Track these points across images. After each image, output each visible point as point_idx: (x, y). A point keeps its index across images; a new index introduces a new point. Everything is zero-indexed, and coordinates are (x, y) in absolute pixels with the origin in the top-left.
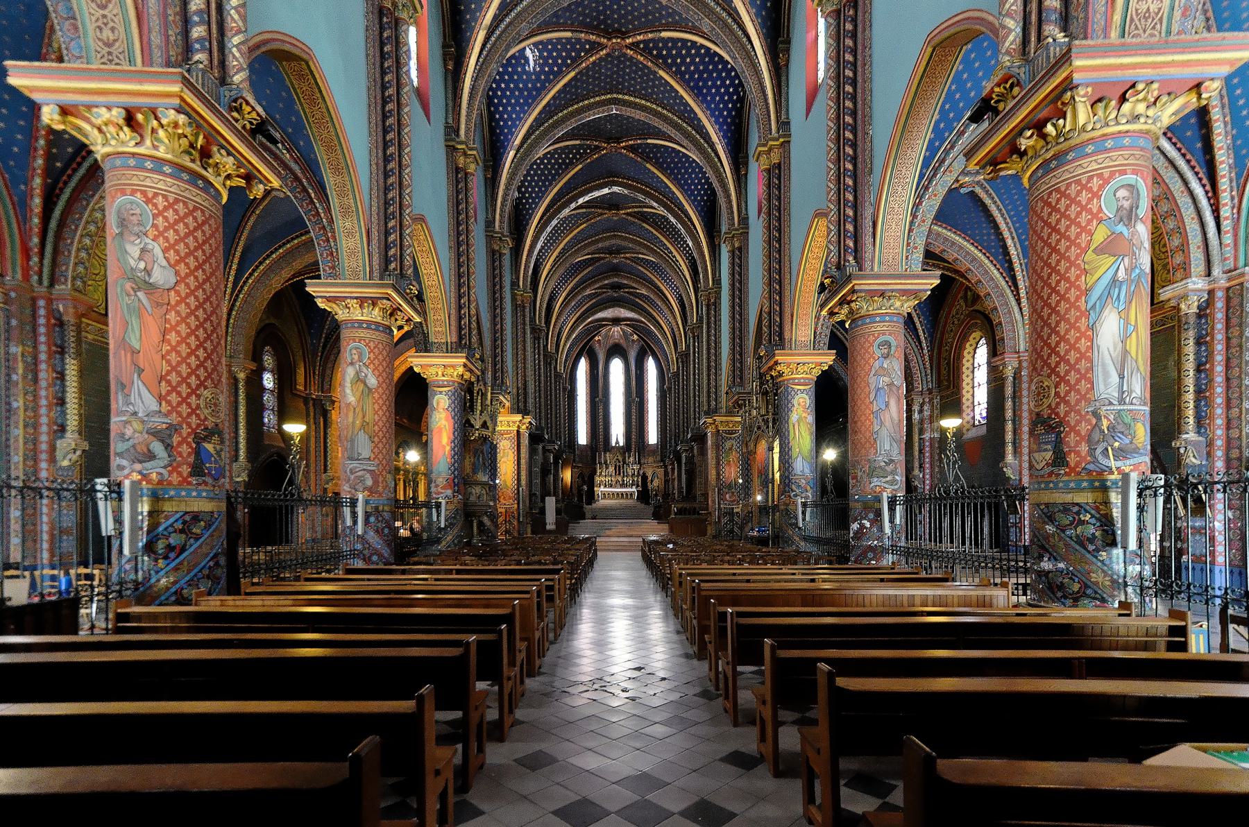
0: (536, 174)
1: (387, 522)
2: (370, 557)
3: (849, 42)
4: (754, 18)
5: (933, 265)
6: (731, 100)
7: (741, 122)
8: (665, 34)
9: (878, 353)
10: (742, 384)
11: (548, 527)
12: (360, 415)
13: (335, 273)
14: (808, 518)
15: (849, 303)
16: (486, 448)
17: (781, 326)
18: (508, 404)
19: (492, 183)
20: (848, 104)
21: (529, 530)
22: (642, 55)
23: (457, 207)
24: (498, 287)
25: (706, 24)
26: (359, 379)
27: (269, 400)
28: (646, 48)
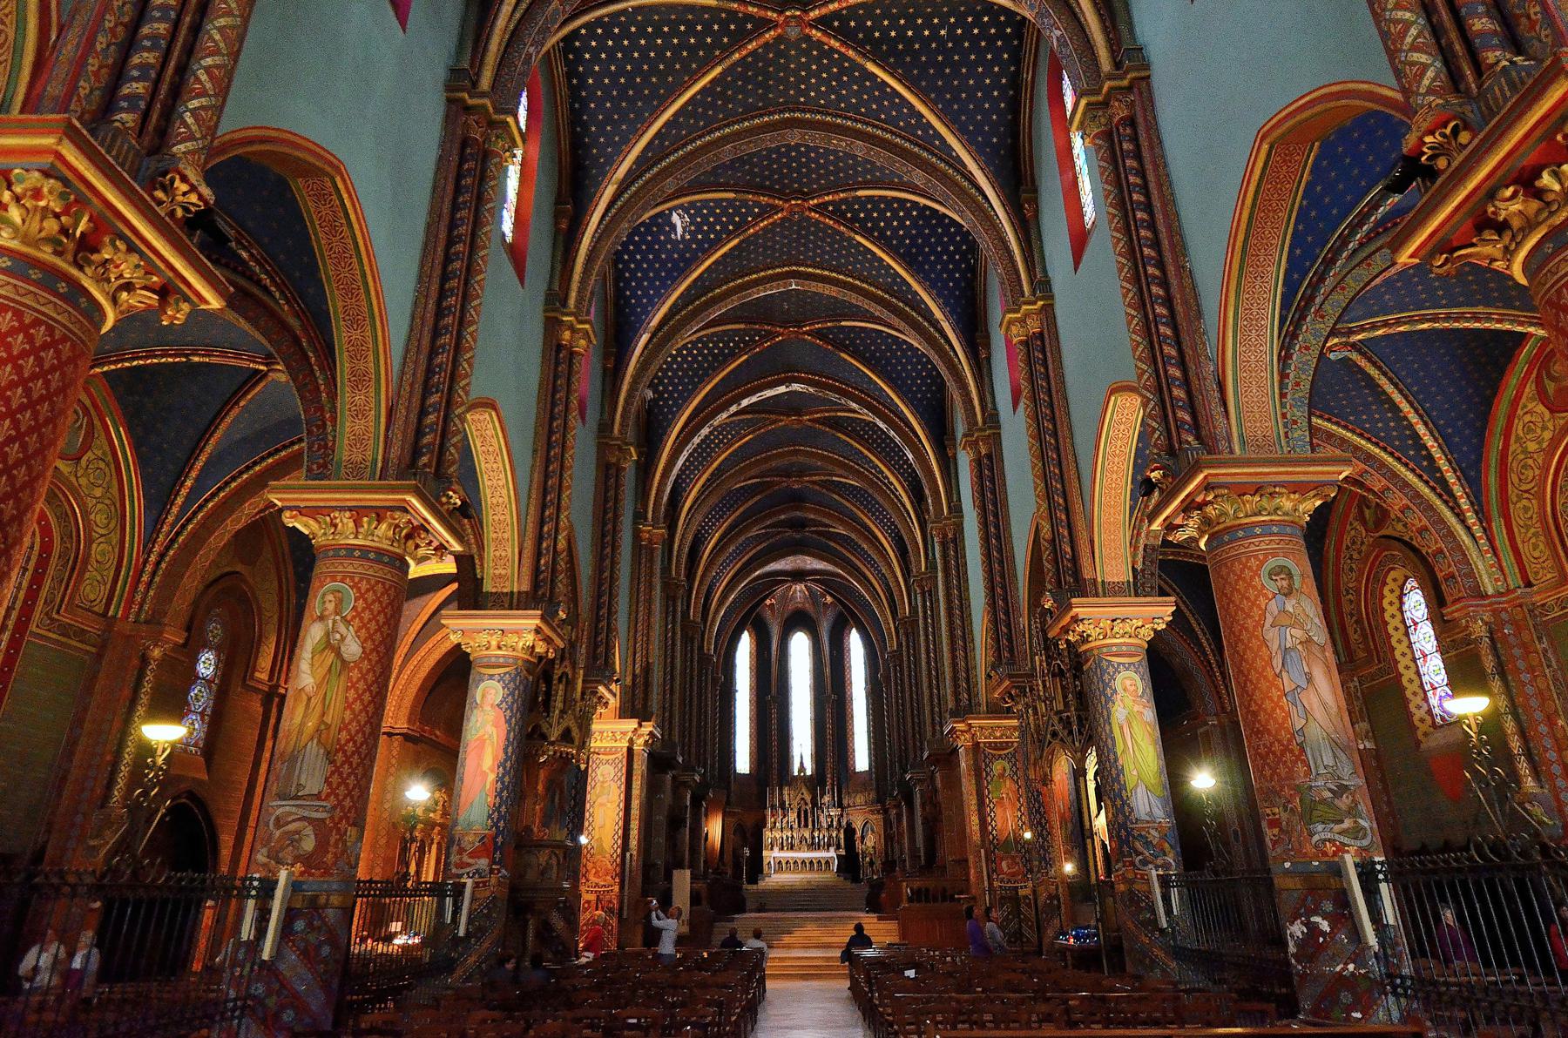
2: (277, 1016)
4: (984, 166)
12: (318, 709)
16: (567, 779)
17: (1075, 559)
19: (612, 375)
22: (830, 219)
23: (553, 395)
24: (610, 515)
25: (918, 177)
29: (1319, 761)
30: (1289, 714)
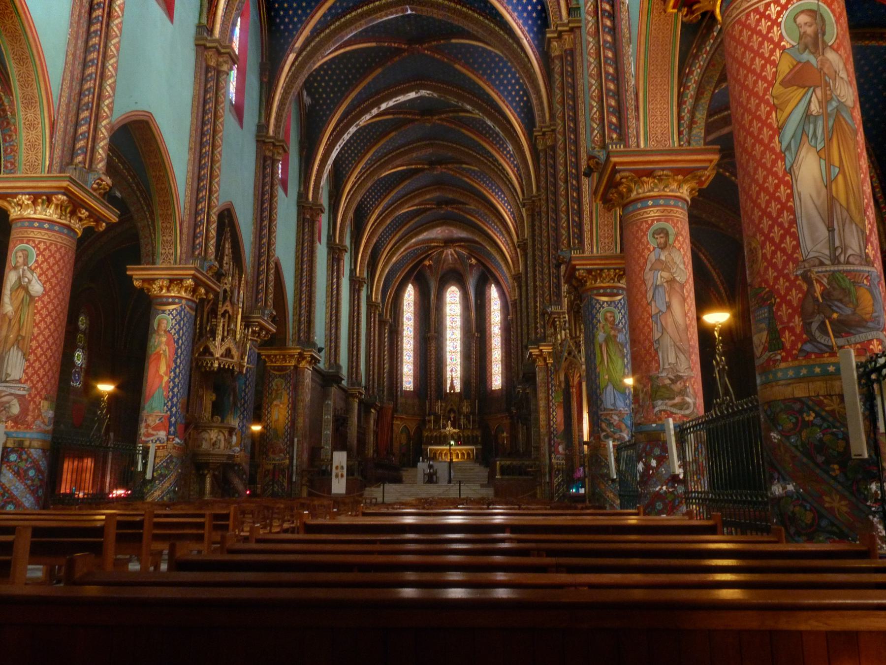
26: (22, 287)
29: (666, 360)
30: (652, 330)
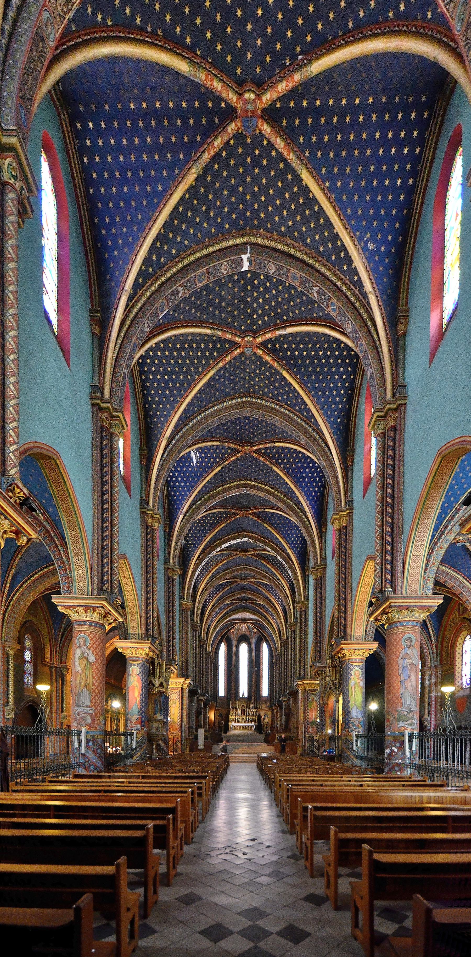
0: (196, 529)
1: (100, 745)
2: (89, 768)
3: (390, 453)
4: (332, 436)
5: (439, 590)
6: (317, 486)
7: (323, 499)
8: (277, 444)
9: (404, 645)
10: (320, 661)
11: (200, 747)
12: (84, 679)
13: (70, 591)
14: (359, 745)
15: (387, 614)
16: (162, 699)
17: (345, 626)
18: (176, 672)
19: (168, 535)
20: (389, 491)
21: (188, 750)
22: (263, 457)
24: (171, 599)
25: (303, 439)
27: (28, 668)
28: (265, 453)
